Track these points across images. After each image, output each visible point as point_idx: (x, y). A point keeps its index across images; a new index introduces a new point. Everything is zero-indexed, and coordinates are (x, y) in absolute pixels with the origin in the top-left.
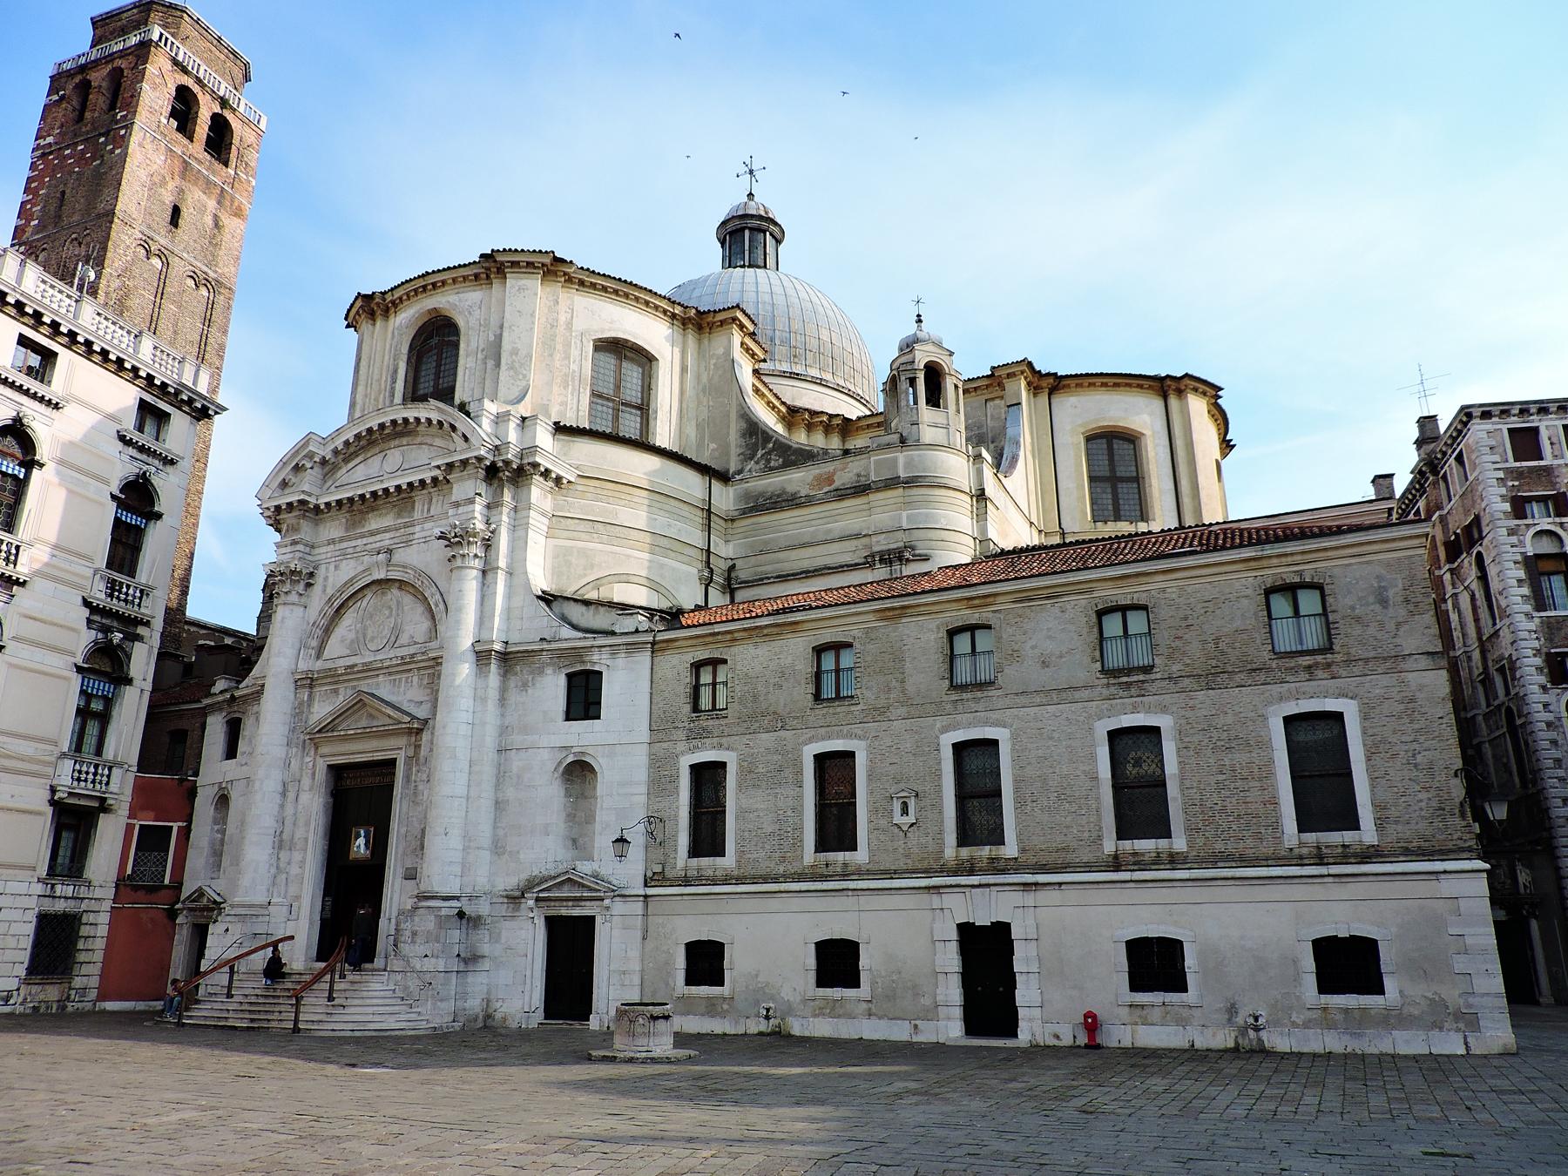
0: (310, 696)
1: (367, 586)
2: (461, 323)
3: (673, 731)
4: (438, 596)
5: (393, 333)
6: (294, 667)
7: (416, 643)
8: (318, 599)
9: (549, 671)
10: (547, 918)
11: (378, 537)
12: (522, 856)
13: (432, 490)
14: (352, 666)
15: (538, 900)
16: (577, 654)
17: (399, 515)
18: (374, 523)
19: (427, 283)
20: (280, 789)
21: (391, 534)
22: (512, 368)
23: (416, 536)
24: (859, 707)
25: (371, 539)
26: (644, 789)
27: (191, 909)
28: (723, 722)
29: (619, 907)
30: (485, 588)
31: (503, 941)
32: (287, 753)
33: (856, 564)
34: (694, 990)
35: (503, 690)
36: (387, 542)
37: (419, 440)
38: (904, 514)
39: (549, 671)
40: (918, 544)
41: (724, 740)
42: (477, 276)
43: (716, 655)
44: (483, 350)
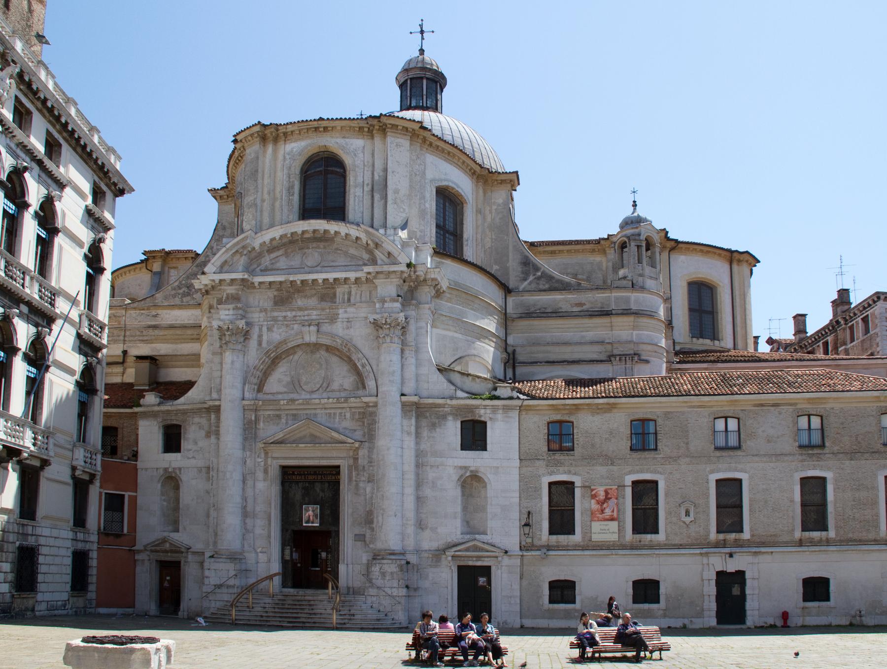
0: (256, 417)
1: (298, 346)
2: (348, 160)
3: (536, 461)
4: (364, 361)
5: (284, 157)
6: (242, 396)
7: (345, 390)
8: (255, 350)
9: (450, 418)
10: (459, 566)
11: (306, 313)
12: (439, 530)
13: (353, 286)
14: (293, 401)
15: (452, 556)
16: (471, 409)
17: (323, 298)
18: (300, 302)
19: (320, 126)
20: (242, 479)
21: (318, 312)
22: (395, 203)
23: (340, 316)
24: (661, 456)
25: (299, 313)
26: (518, 495)
27: (152, 551)
28: (572, 458)
29: (506, 561)
30: (404, 360)
31: (431, 578)
32: (243, 455)
33: (601, 361)
34: (556, 606)
35: (417, 428)
36: (314, 317)
37: (335, 246)
38: (635, 333)
39: (450, 418)
40: (643, 353)
41: (572, 469)
42: (361, 129)
43: (566, 418)
44: (368, 185)
